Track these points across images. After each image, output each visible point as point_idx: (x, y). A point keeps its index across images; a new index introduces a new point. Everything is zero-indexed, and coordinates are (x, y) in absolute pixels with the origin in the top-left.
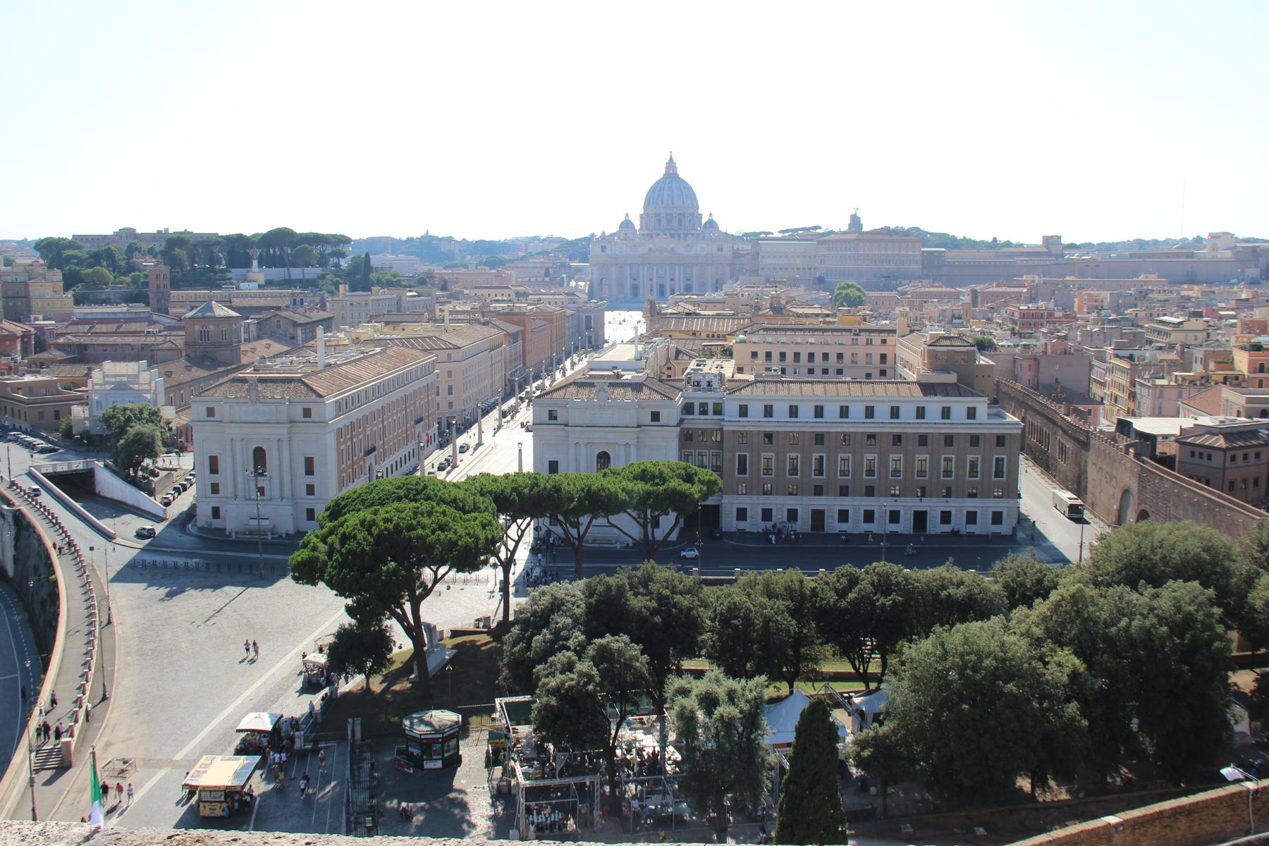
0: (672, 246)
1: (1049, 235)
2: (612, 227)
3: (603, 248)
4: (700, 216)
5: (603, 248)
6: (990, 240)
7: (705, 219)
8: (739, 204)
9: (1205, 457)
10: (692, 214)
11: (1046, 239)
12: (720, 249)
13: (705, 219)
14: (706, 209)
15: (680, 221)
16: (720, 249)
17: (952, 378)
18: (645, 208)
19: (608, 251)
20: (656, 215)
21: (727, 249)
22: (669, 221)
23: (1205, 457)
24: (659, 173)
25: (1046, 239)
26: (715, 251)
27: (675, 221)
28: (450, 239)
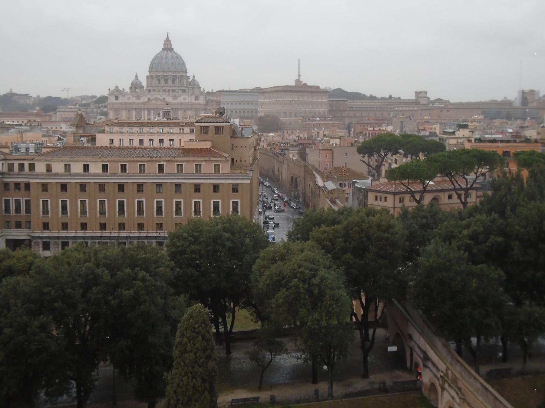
0: (164, 96)
1: (418, 90)
2: (125, 85)
3: (117, 98)
4: (188, 77)
5: (117, 98)
6: (388, 97)
7: (191, 79)
8: (216, 71)
9: (383, 199)
10: (182, 76)
11: (417, 93)
12: (197, 99)
13: (191, 79)
14: (190, 74)
15: (173, 81)
16: (197, 99)
17: (207, 145)
18: (150, 72)
19: (120, 100)
20: (157, 76)
21: (202, 100)
22: (166, 81)
23: (383, 199)
24: (159, 47)
25: (417, 93)
26: (193, 100)
27: (170, 81)
28: (27, 96)
